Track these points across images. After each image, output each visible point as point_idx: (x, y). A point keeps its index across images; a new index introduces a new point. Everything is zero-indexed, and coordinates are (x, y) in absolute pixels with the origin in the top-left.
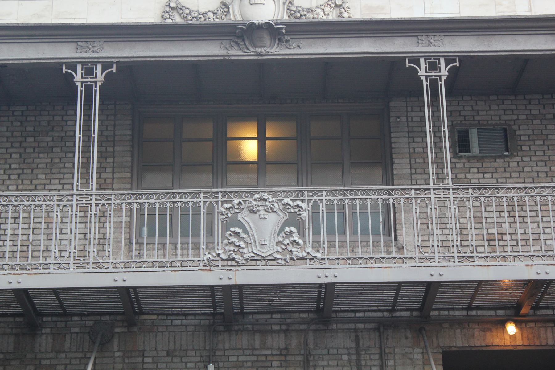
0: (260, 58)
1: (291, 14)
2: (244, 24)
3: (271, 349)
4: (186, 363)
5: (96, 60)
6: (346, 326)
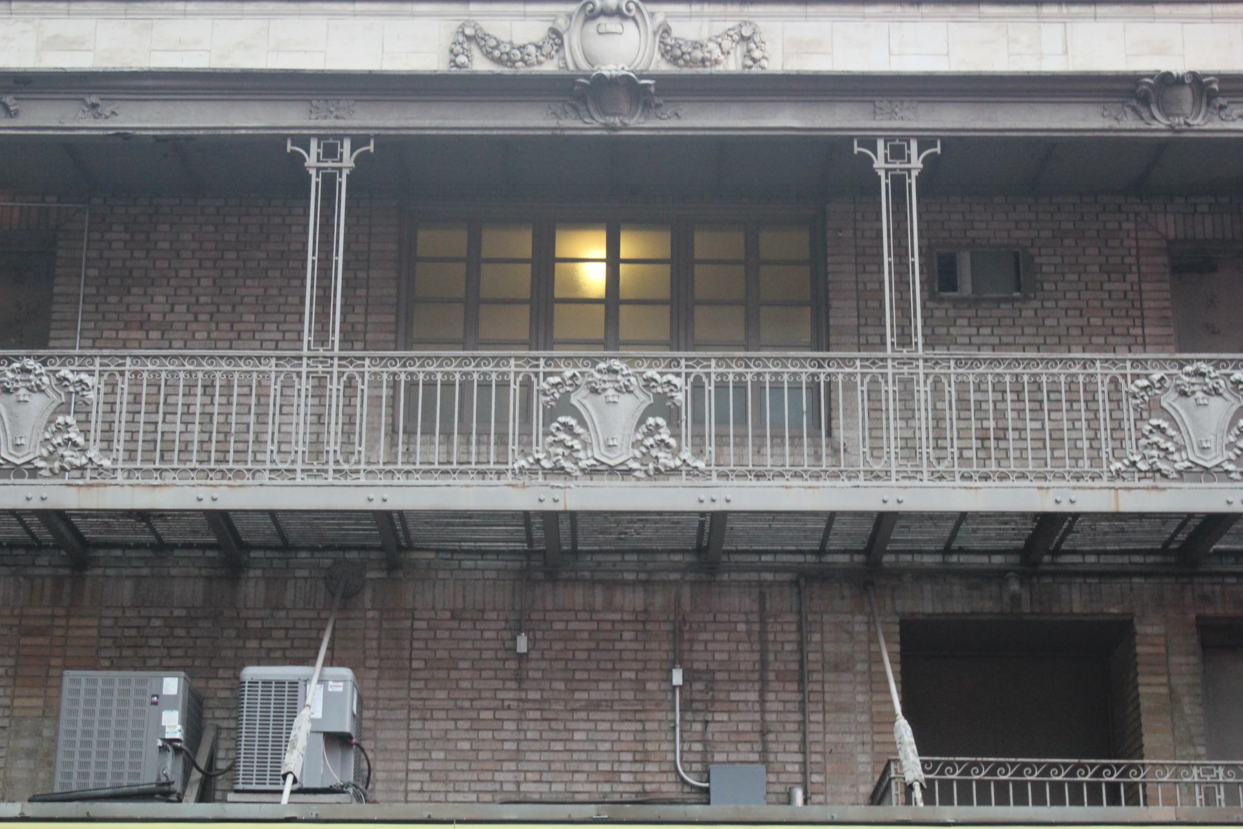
0: (612, 133)
1: (667, 52)
2: (587, 77)
3: (622, 611)
4: (482, 631)
5: (342, 132)
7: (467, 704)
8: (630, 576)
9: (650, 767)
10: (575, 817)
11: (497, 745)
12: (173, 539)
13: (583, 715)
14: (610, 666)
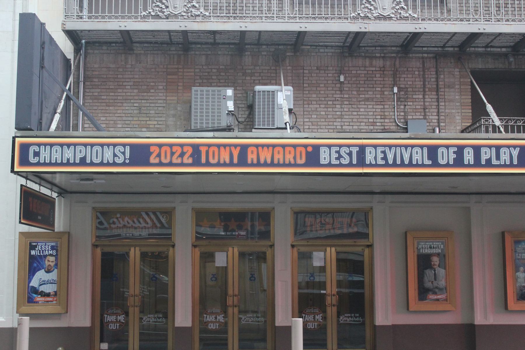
4: (328, 74)
6: (417, 55)
7: (323, 99)
8: (378, 55)
9: (386, 121)
10: (402, 137)
11: (334, 113)
12: (219, 41)
13: (363, 103)
14: (372, 86)
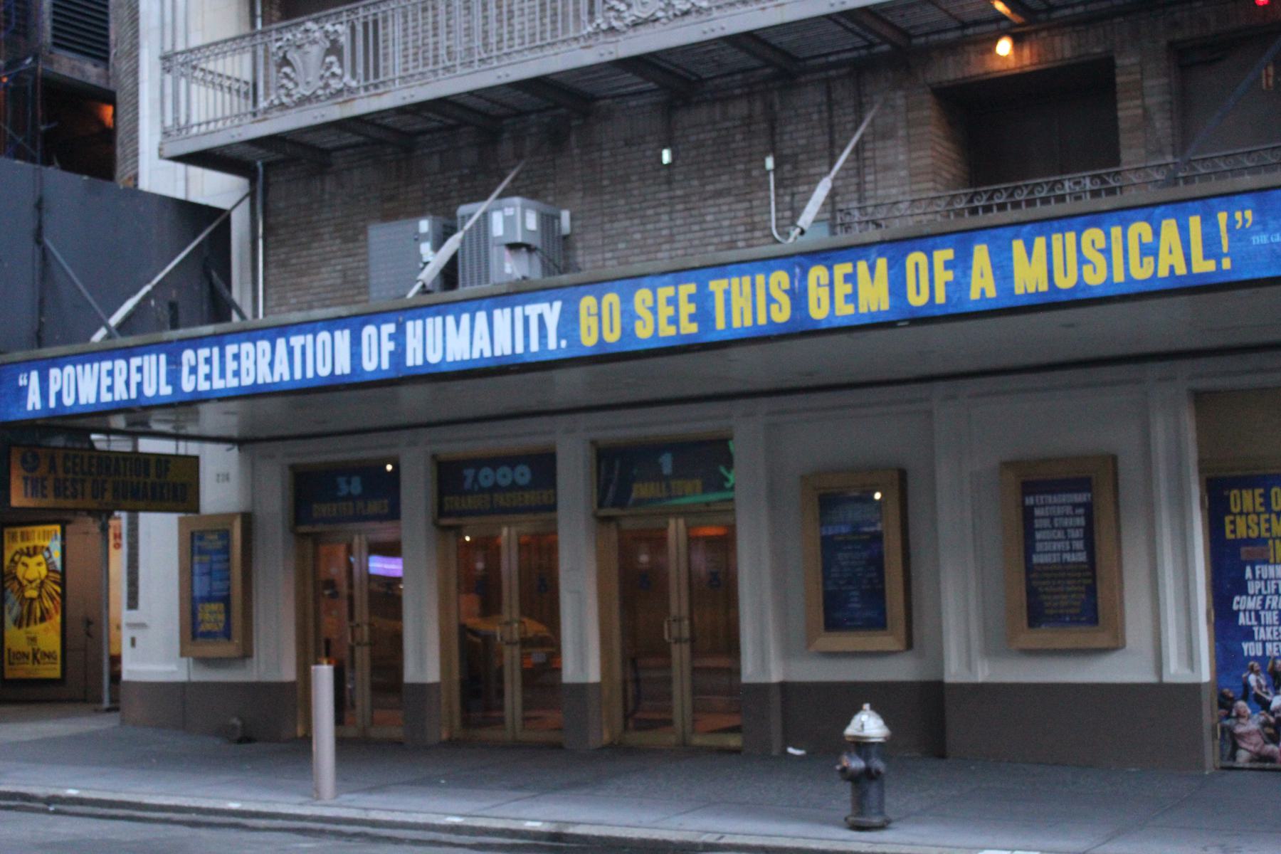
7: (637, 206)
